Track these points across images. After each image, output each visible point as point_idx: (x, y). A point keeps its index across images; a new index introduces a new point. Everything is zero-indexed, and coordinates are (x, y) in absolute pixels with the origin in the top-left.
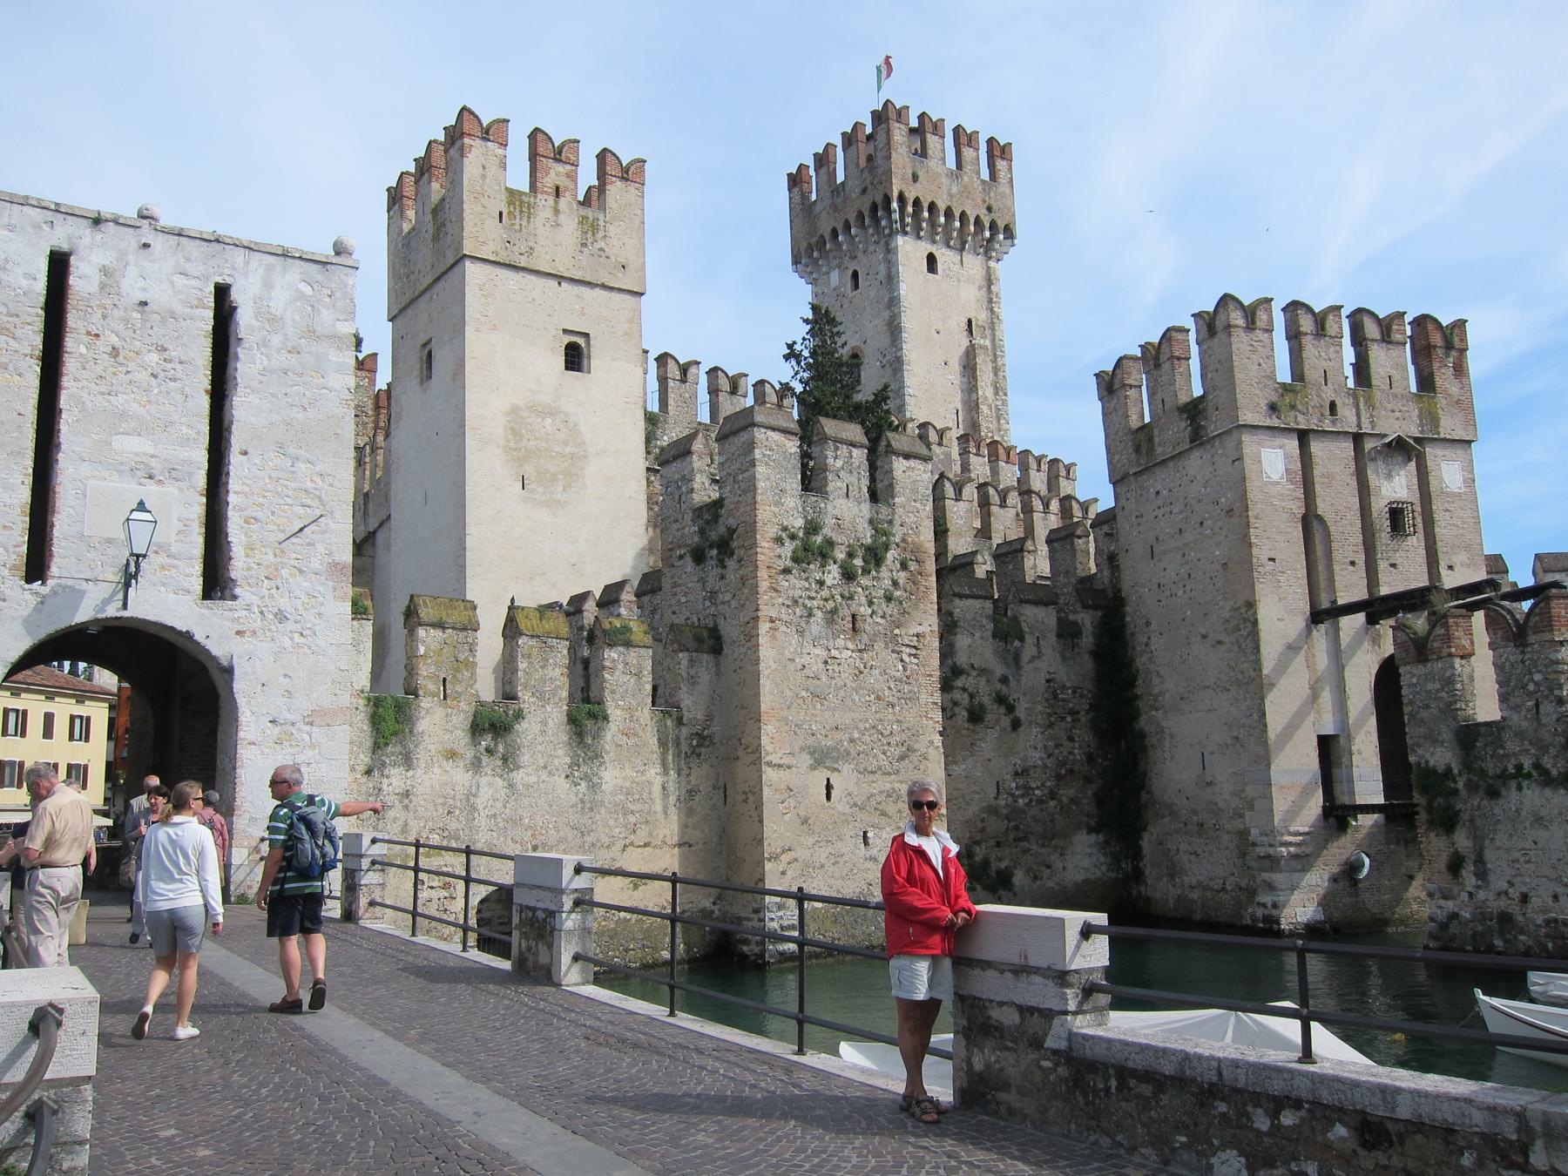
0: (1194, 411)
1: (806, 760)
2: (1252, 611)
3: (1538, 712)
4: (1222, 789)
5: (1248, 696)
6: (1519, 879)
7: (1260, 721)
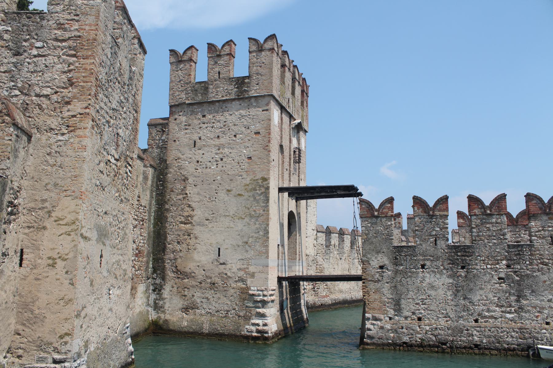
0: (241, 82)
1: (93, 235)
2: (266, 182)
3: (436, 244)
4: (232, 266)
5: (257, 223)
6: (417, 311)
7: (264, 236)
